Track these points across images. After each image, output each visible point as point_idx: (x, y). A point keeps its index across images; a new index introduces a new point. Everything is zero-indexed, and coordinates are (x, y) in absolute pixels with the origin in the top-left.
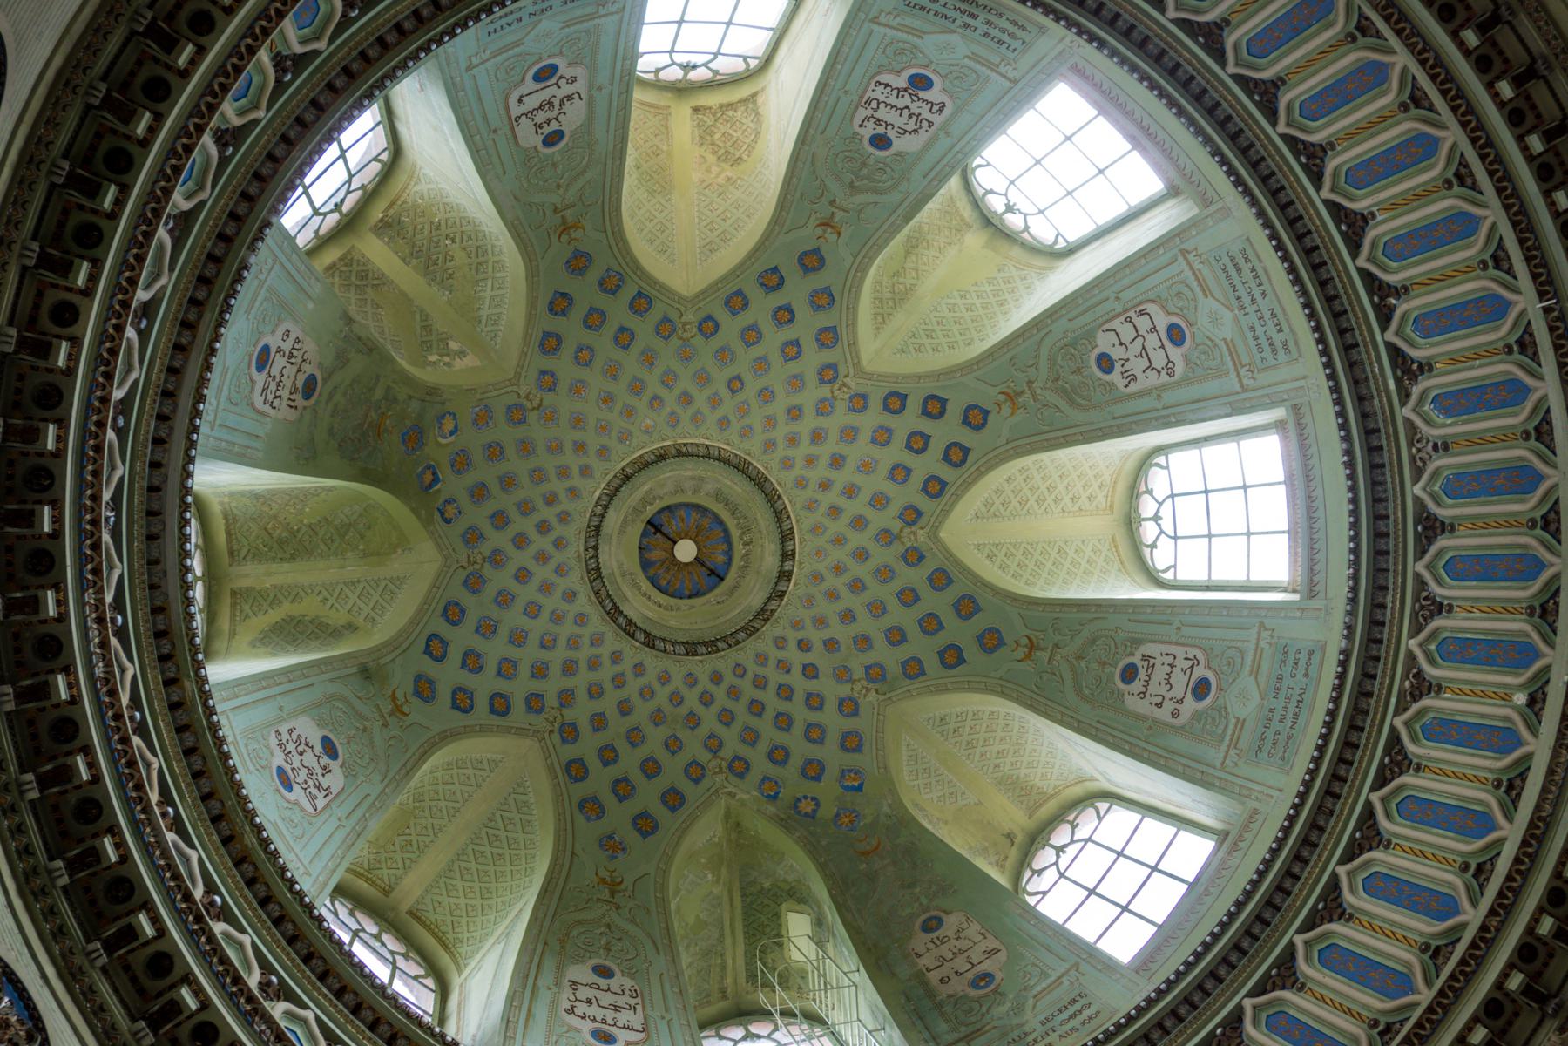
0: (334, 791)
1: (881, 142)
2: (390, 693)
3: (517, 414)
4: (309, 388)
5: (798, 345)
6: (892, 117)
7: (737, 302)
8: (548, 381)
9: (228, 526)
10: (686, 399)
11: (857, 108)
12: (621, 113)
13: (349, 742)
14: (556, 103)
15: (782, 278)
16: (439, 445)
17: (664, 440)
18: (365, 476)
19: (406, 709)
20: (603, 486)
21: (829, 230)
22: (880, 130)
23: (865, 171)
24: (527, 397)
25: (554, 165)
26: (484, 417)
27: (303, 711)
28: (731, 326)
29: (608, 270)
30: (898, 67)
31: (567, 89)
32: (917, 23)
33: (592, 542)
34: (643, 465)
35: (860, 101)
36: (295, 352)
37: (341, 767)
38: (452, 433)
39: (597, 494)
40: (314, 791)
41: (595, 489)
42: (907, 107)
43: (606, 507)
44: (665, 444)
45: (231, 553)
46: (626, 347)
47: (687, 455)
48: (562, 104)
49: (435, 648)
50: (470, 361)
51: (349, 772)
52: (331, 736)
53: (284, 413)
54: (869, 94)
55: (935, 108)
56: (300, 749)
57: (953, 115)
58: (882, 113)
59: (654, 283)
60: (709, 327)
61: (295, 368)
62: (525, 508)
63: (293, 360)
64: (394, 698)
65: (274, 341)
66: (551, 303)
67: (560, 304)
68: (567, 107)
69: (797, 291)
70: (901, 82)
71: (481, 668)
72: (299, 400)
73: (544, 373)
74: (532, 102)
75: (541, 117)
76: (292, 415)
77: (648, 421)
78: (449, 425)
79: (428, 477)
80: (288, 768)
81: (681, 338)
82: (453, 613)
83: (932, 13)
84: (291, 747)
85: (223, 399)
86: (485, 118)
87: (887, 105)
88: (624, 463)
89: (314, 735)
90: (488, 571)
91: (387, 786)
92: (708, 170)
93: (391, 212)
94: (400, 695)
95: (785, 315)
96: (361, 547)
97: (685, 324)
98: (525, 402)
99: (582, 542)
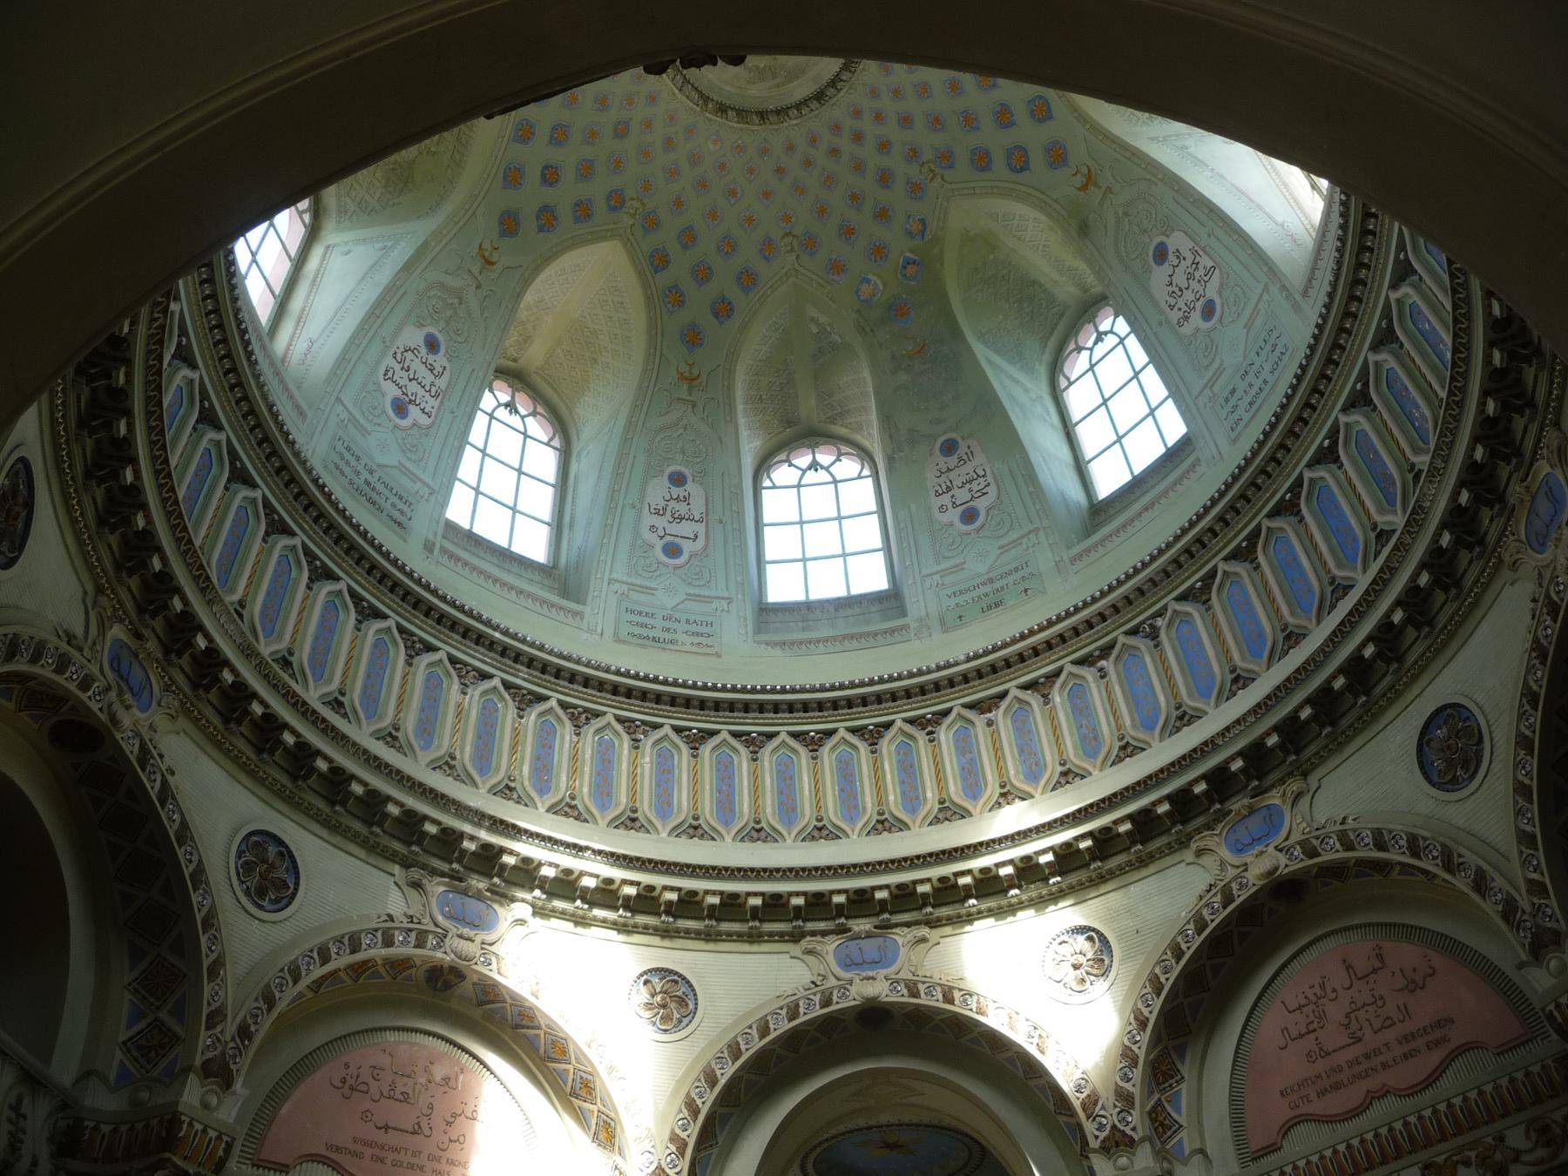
0: (1192, 244)
1: (432, 345)
2: (1082, 193)
3: (810, 244)
4: (949, 448)
5: (551, 137)
6: (423, 372)
7: (583, 211)
8: (767, 249)
9: (1049, 338)
10: (669, 143)
11: (448, 387)
12: (621, 471)
13: (1145, 231)
14: (668, 513)
15: (538, 217)
16: (885, 285)
17: (710, 120)
18: (957, 333)
19: (1085, 170)
20: (785, 124)
21: (487, 254)
22: (431, 358)
23: (449, 313)
24: (792, 250)
25: (683, 453)
26: (837, 267)
27: (1146, 290)
28: (596, 190)
29: (672, 313)
30: (414, 431)
31: (660, 522)
32: (404, 481)
33: (830, 92)
34: (742, 114)
35: (444, 396)
36: (944, 487)
37: (1168, 236)
38: (869, 281)
39: (795, 122)
40: (1201, 272)
41: (794, 129)
42: (410, 380)
43: (798, 106)
44: (710, 116)
45: (1062, 315)
46: (690, 228)
47: (701, 94)
48: (665, 509)
49: (1019, 161)
50: (815, 313)
51: (1168, 228)
52: (1151, 253)
53: (980, 458)
54: (436, 403)
55: (390, 374)
56: (1177, 290)
57: (378, 363)
58: (428, 378)
59: (641, 274)
60: (616, 201)
61: (952, 475)
62: (859, 166)
63: (949, 484)
64: (1084, 188)
65: (953, 515)
66: (729, 316)
67: (723, 309)
68: (662, 504)
69: (531, 195)
70: (414, 411)
71: (1002, 105)
72: (962, 450)
73: (766, 259)
74: (686, 528)
75: (682, 509)
76: (976, 448)
77: (711, 147)
78: (866, 290)
79: (911, 270)
80: (1199, 305)
81: (643, 204)
82: (981, 160)
83: (394, 492)
84: (1181, 304)
85: (1014, 535)
86: (725, 542)
87: (423, 387)
88: (755, 128)
89: (1160, 274)
90: (928, 155)
91: (1155, 177)
92: (537, 319)
93: (781, 430)
94: (1079, 181)
95: (550, 176)
96: (992, 257)
97: (633, 216)
98: (796, 247)
99: (838, 96)
